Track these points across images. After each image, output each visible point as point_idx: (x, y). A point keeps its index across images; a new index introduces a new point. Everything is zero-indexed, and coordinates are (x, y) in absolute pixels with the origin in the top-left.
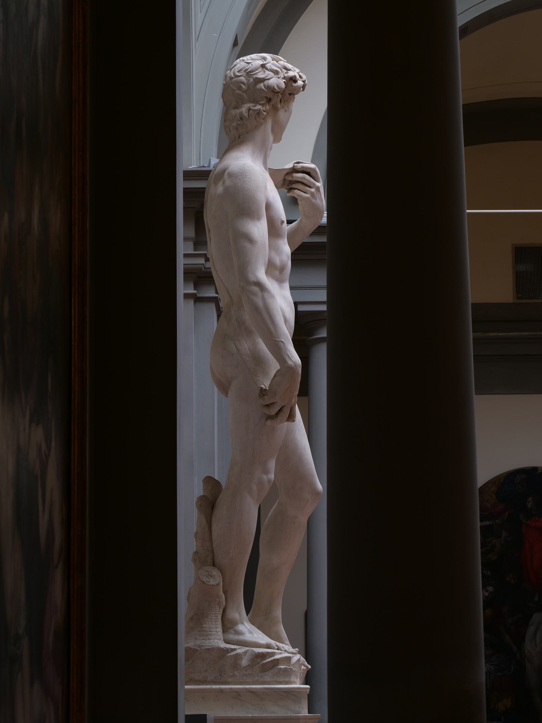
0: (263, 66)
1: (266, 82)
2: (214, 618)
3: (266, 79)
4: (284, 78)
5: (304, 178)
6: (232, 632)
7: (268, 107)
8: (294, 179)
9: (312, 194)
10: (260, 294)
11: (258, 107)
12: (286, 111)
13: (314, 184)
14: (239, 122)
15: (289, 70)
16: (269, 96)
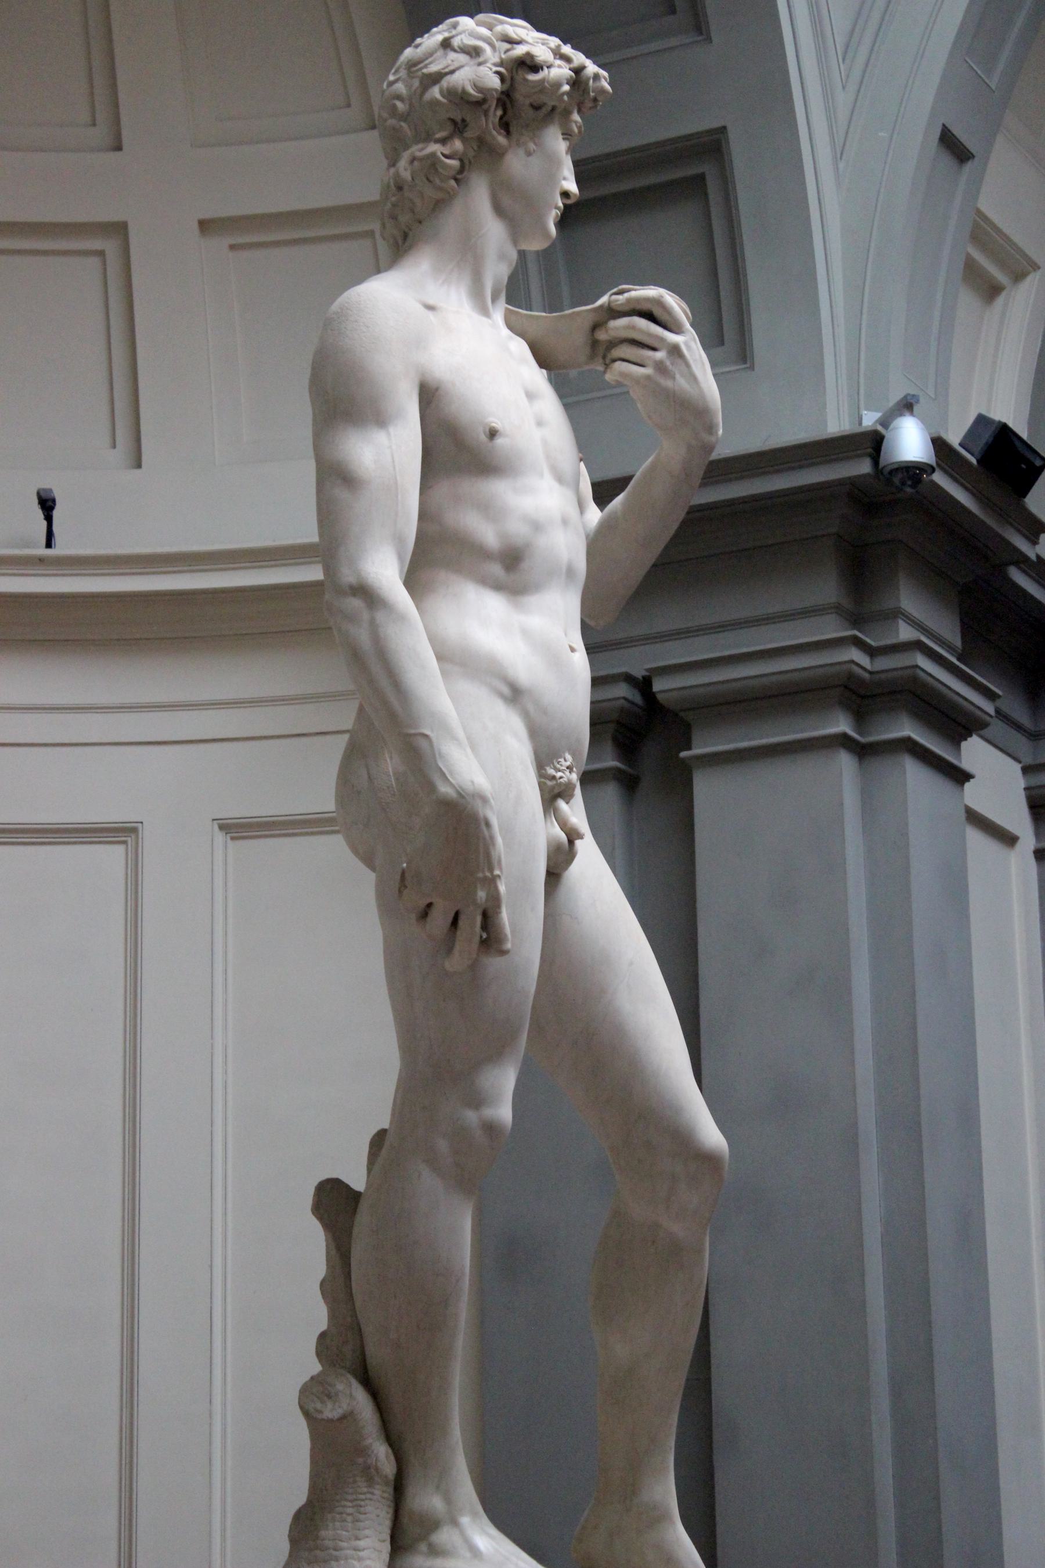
0: (446, 44)
1: (445, 83)
2: (350, 1510)
3: (447, 74)
4: (501, 64)
5: (633, 327)
6: (423, 1547)
7: (458, 145)
8: (613, 334)
9: (660, 367)
10: (365, 615)
11: (434, 148)
12: (529, 154)
13: (662, 340)
14: (393, 199)
15: (519, 43)
16: (458, 119)
